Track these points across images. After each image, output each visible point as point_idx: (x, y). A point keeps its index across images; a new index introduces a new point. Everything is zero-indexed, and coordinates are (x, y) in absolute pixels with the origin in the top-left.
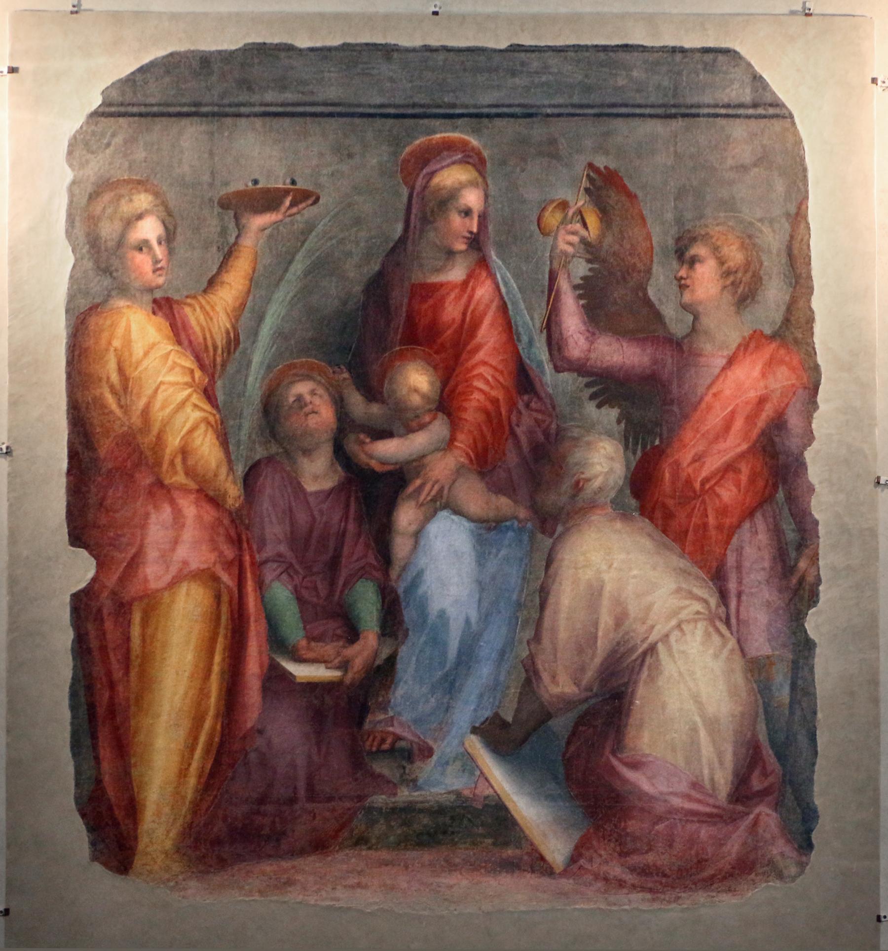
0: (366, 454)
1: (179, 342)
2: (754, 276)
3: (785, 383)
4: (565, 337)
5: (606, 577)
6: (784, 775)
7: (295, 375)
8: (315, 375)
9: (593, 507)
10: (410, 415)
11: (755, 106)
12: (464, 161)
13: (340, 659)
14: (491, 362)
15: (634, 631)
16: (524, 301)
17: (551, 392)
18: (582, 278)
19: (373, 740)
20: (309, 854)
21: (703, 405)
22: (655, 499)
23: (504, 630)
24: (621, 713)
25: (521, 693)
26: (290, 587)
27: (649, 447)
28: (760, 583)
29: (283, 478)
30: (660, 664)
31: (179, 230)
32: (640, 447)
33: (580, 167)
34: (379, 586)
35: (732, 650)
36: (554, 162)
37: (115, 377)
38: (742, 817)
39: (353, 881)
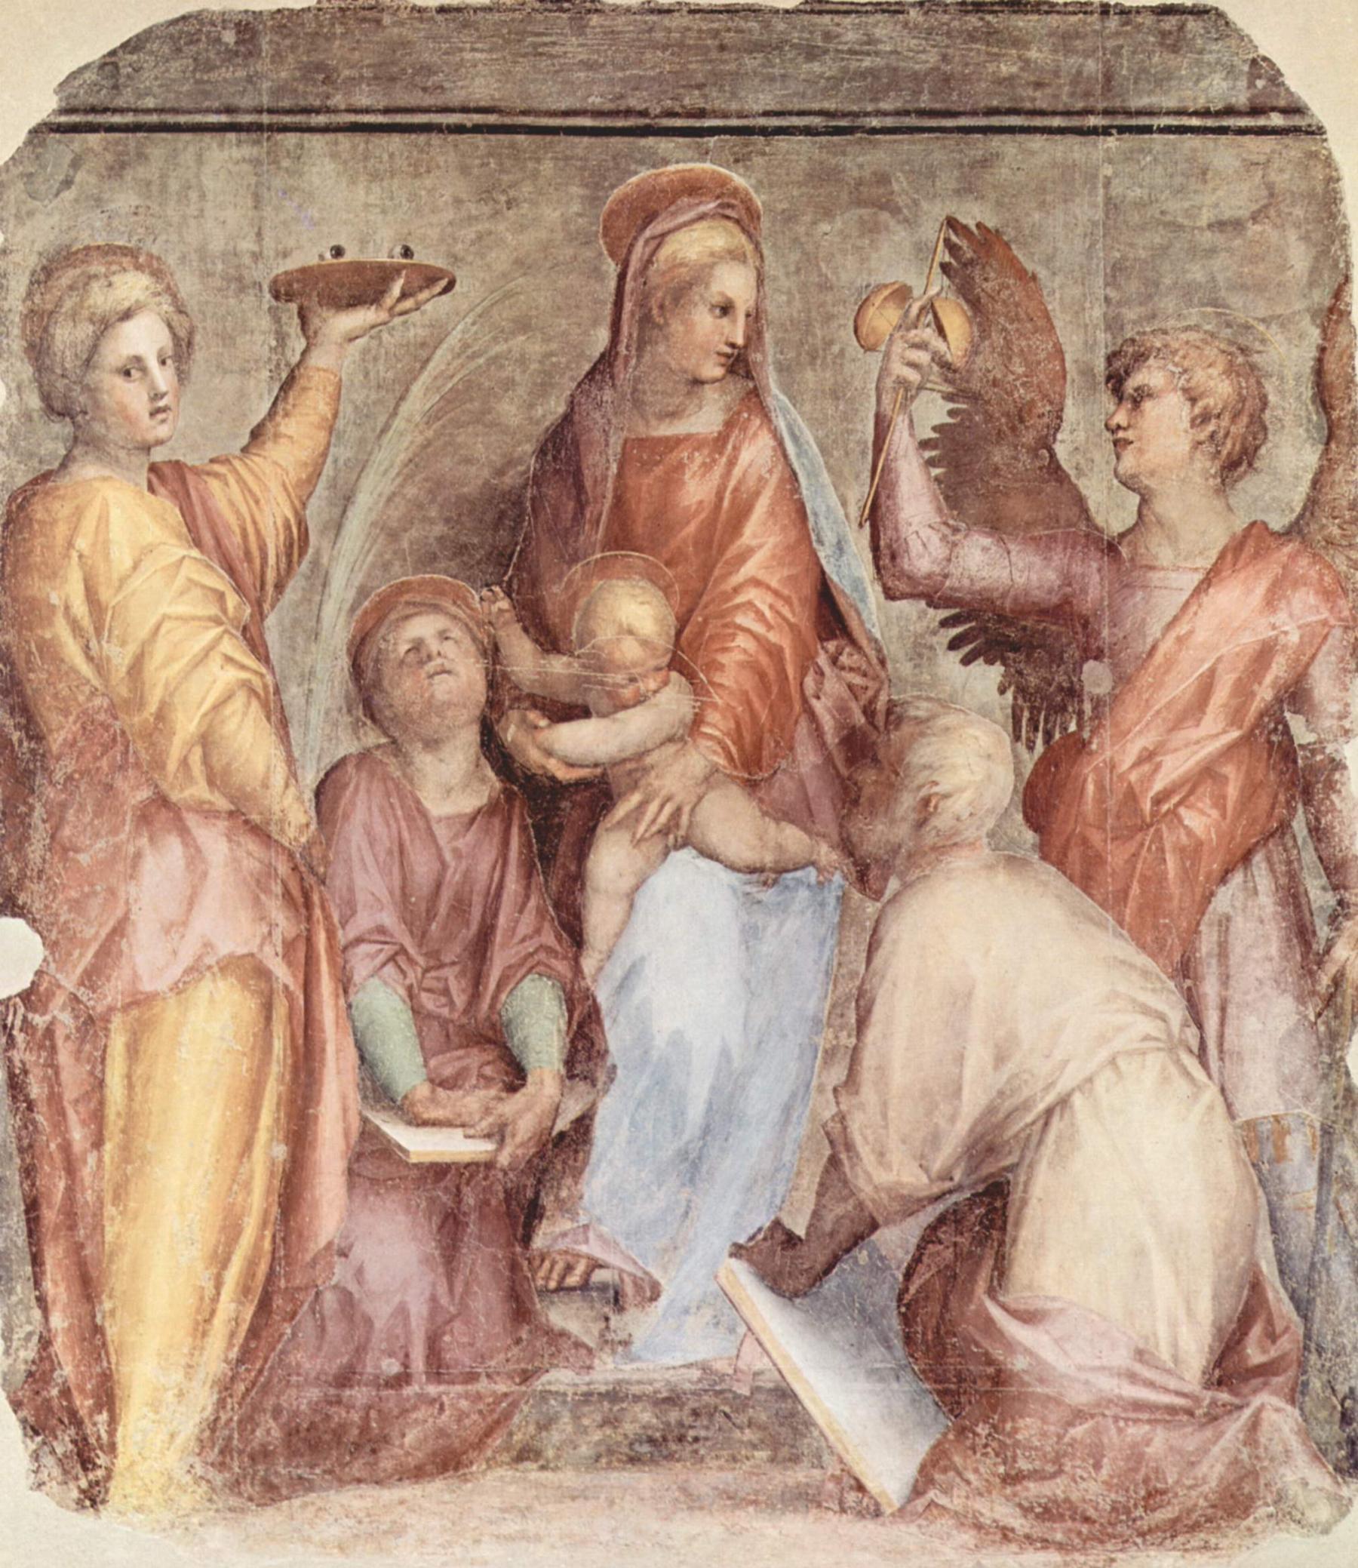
1: (198, 543)
6: (1308, 1336)
7: (408, 603)
8: (447, 604)
10: (620, 678)
11: (1255, 111)
12: (721, 215)
13: (491, 1119)
17: (878, 636)
18: (935, 429)
19: (551, 1270)
20: (432, 1476)
21: (1158, 658)
22: (1069, 829)
23: (793, 1067)
24: (1005, 1222)
25: (822, 1184)
27: (1057, 736)
28: (1260, 982)
31: (198, 338)
32: (1040, 735)
33: (931, 230)
35: (1211, 1108)
36: (885, 216)
37: (80, 609)
38: (1230, 1412)
39: (512, 1526)
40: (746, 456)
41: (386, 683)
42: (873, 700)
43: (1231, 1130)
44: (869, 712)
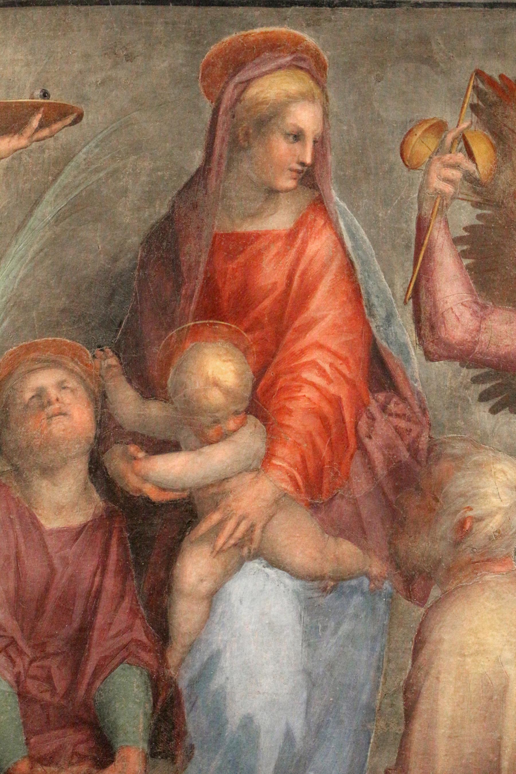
0: (137, 475)
7: (34, 360)
9: (488, 560)
10: (206, 420)
14: (329, 345)
16: (380, 260)
17: (420, 388)
18: (466, 229)
23: (347, 751)
26: (9, 677)
29: (8, 508)
34: (150, 676)
36: (425, 68)
40: (313, 247)
41: (12, 425)
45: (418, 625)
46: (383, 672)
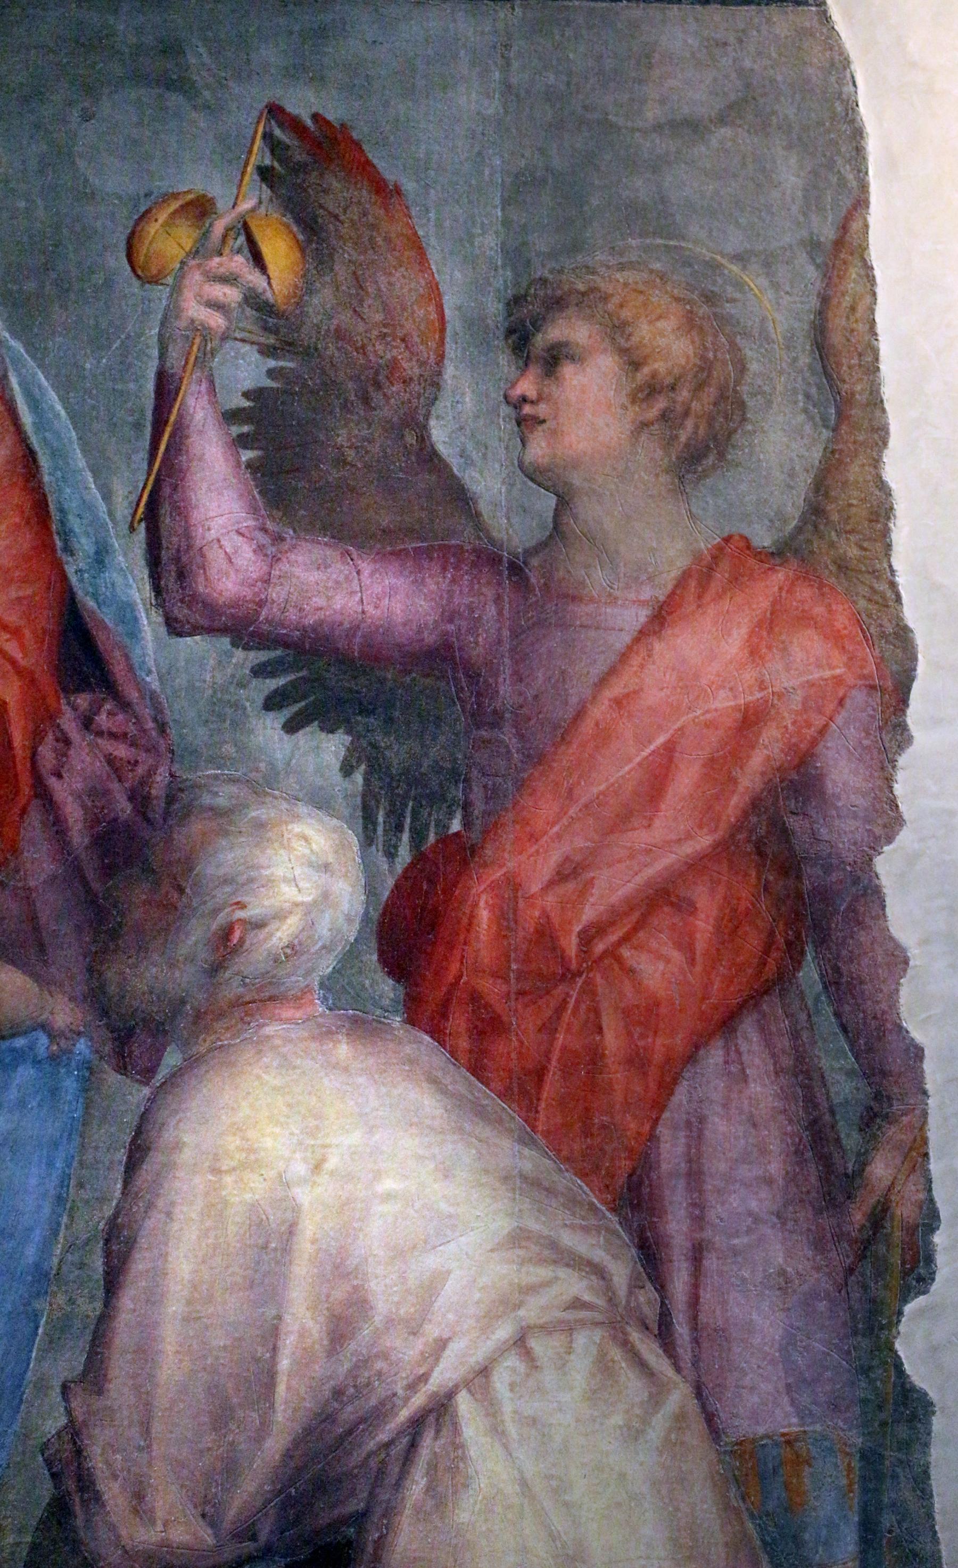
2: (722, 396)
3: (816, 675)
4: (198, 543)
5: (304, 1196)
9: (272, 998)
15: (385, 1356)
17: (156, 686)
18: (246, 395)
21: (587, 727)
22: (450, 978)
27: (432, 838)
28: (757, 1220)
30: (463, 1458)
32: (406, 837)
35: (680, 1418)
36: (175, 99)
42: (145, 781)
43: (713, 1456)
44: (140, 798)
45: (137, 1118)
46: (68, 1206)
